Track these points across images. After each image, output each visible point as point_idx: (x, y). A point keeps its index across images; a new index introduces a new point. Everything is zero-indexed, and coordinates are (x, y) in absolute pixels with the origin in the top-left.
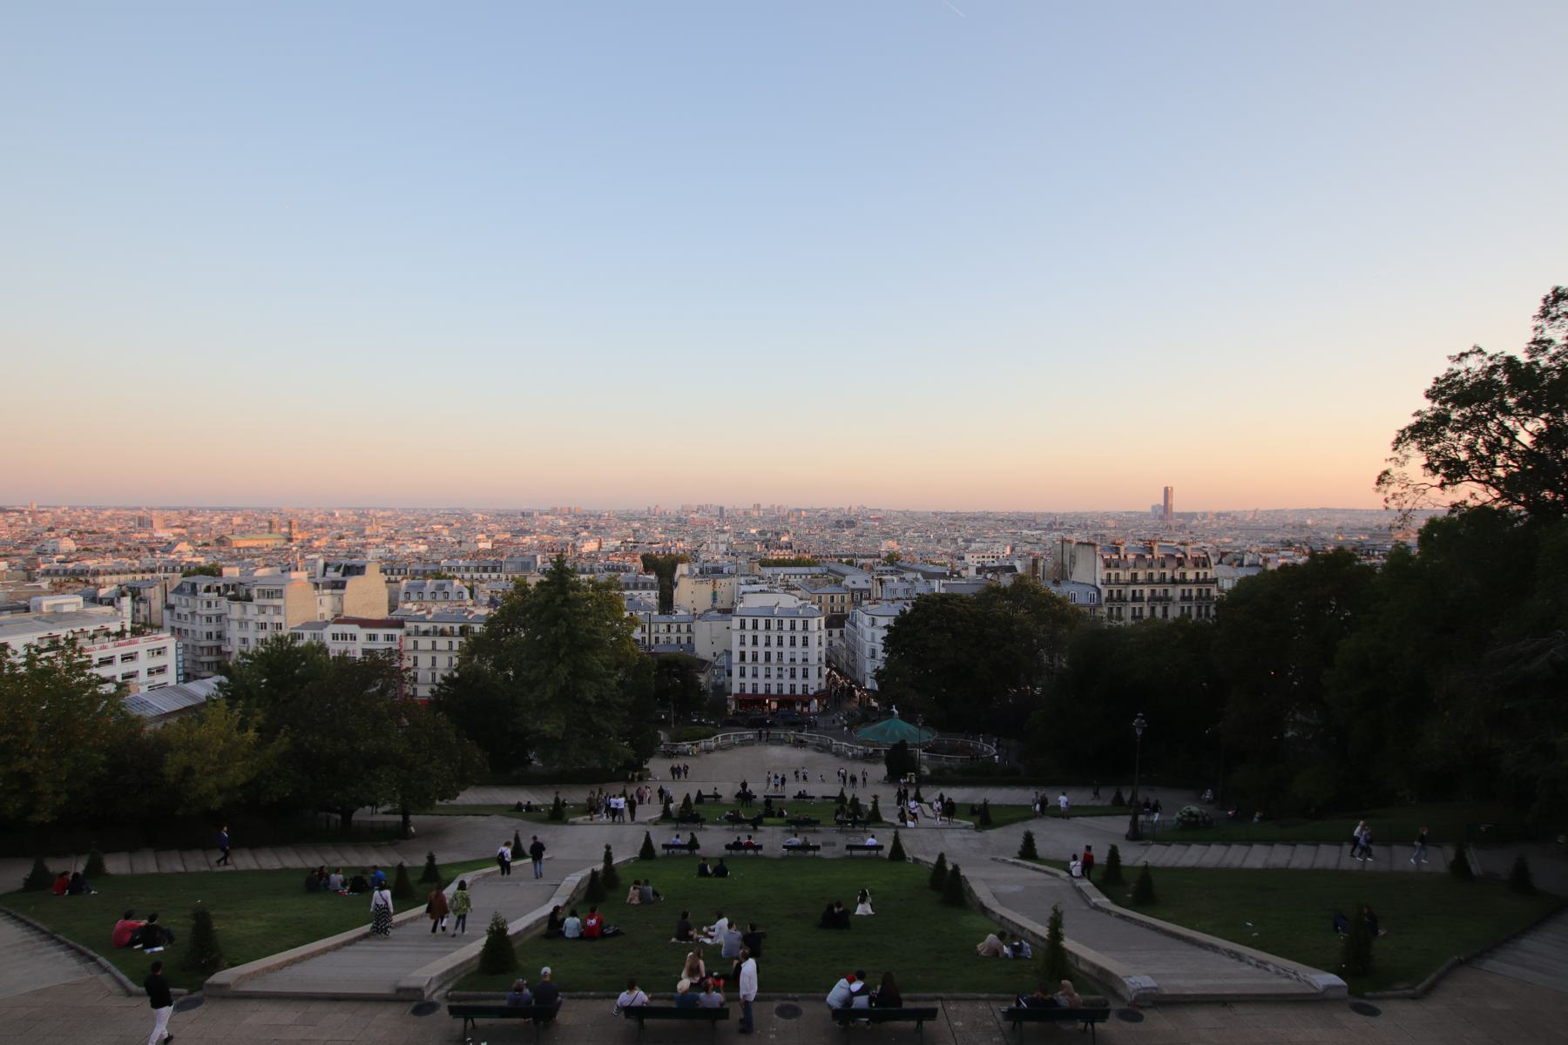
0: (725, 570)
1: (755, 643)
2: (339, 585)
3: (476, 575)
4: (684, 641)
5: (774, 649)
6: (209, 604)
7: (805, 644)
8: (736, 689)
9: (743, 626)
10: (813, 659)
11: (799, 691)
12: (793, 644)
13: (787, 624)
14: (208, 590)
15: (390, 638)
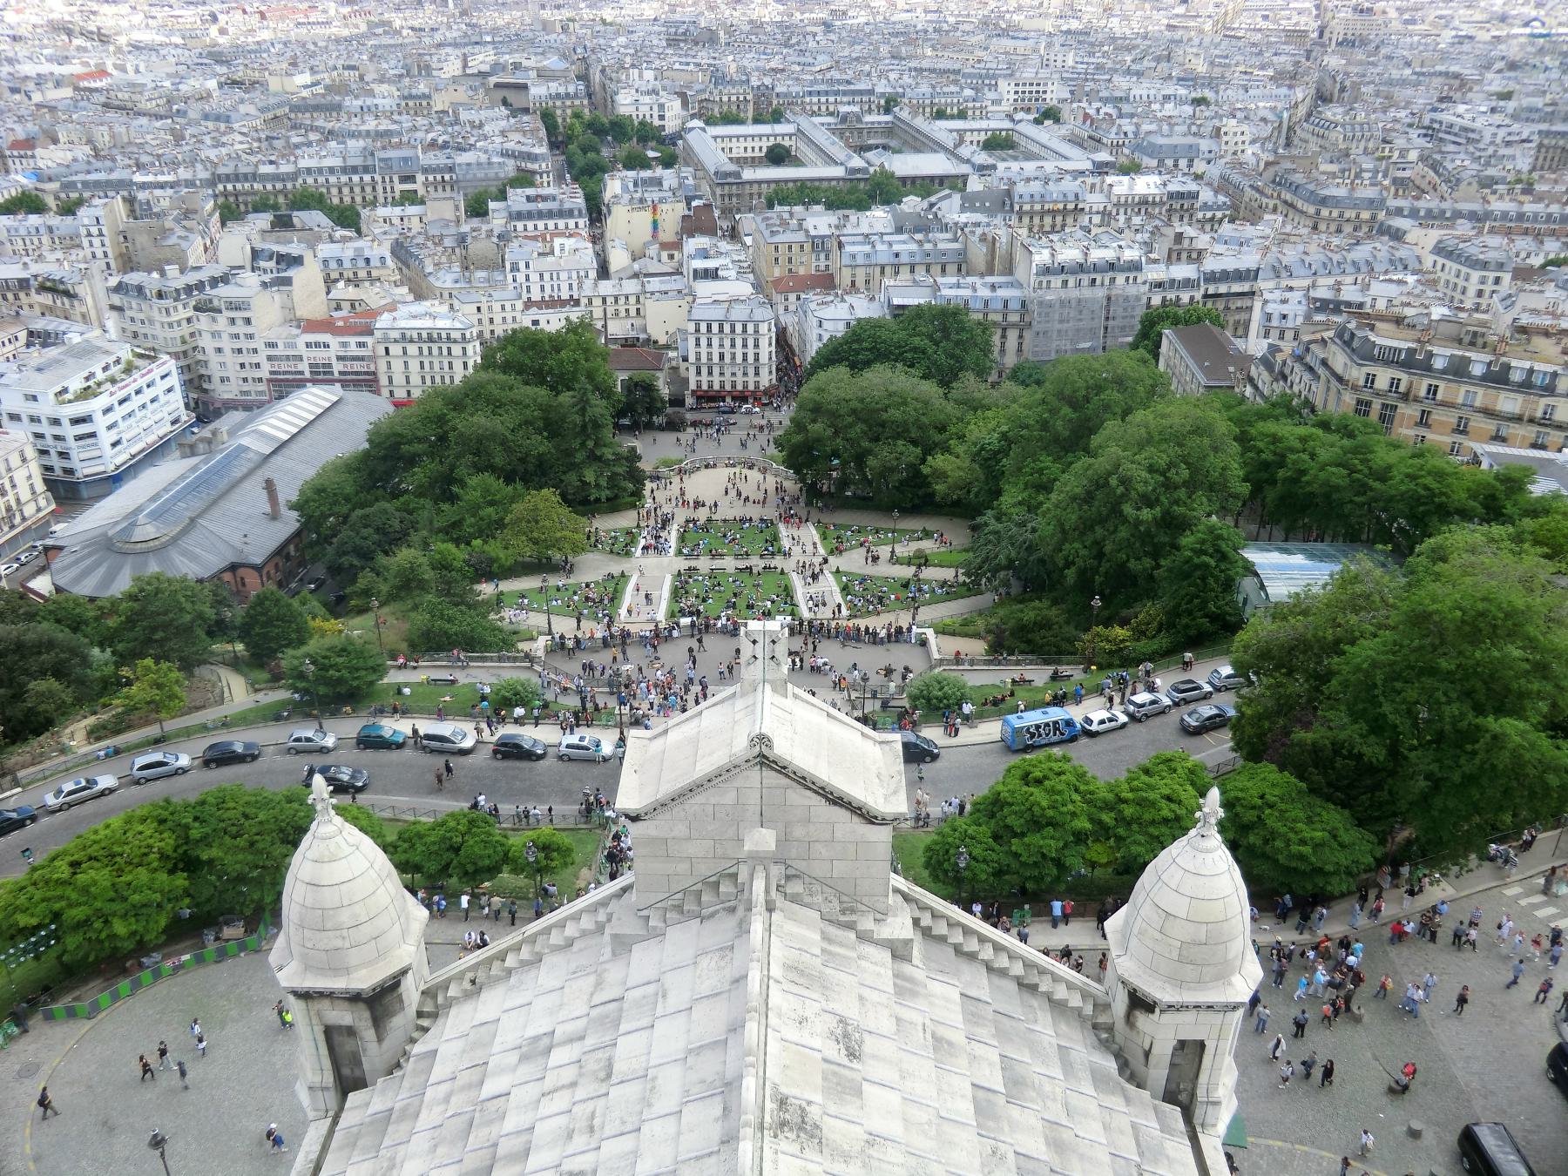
0: (666, 185)
1: (710, 345)
2: (287, 282)
3: (344, 179)
4: (633, 312)
5: (727, 350)
6: (167, 311)
7: (756, 346)
8: (693, 386)
9: (698, 330)
10: (764, 358)
11: (751, 387)
12: (745, 346)
13: (739, 328)
14: (160, 295)
15: (361, 345)
